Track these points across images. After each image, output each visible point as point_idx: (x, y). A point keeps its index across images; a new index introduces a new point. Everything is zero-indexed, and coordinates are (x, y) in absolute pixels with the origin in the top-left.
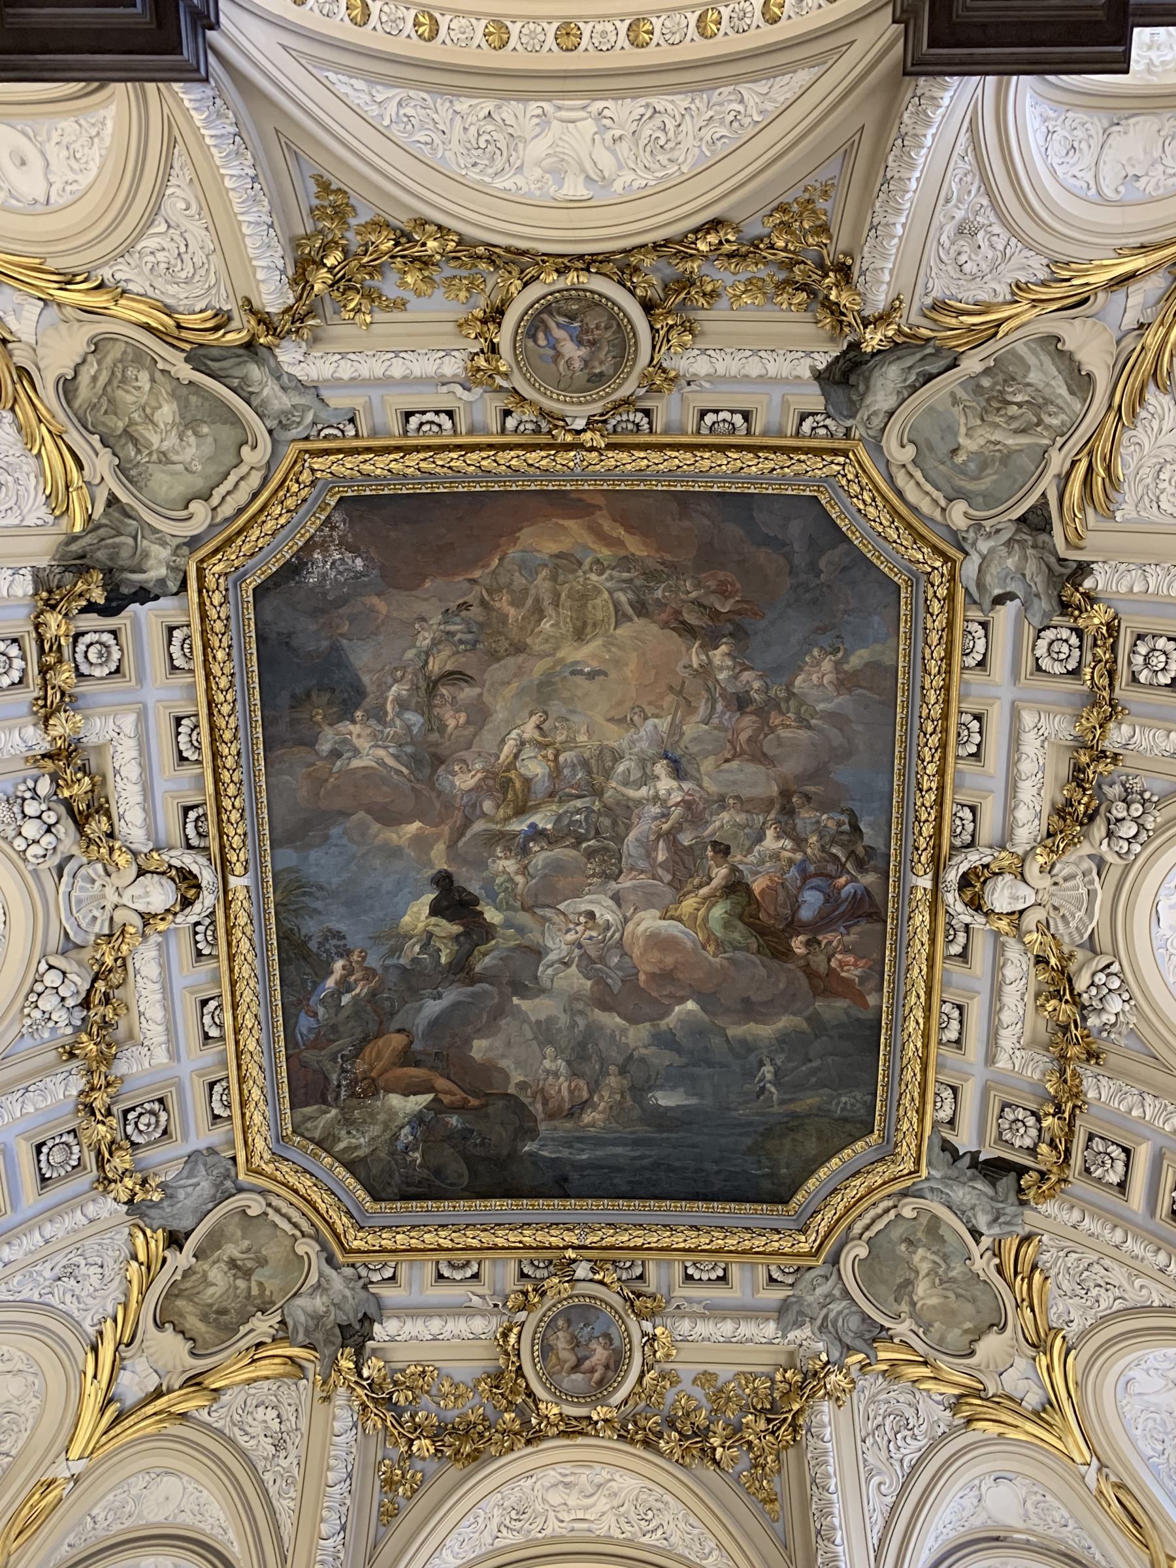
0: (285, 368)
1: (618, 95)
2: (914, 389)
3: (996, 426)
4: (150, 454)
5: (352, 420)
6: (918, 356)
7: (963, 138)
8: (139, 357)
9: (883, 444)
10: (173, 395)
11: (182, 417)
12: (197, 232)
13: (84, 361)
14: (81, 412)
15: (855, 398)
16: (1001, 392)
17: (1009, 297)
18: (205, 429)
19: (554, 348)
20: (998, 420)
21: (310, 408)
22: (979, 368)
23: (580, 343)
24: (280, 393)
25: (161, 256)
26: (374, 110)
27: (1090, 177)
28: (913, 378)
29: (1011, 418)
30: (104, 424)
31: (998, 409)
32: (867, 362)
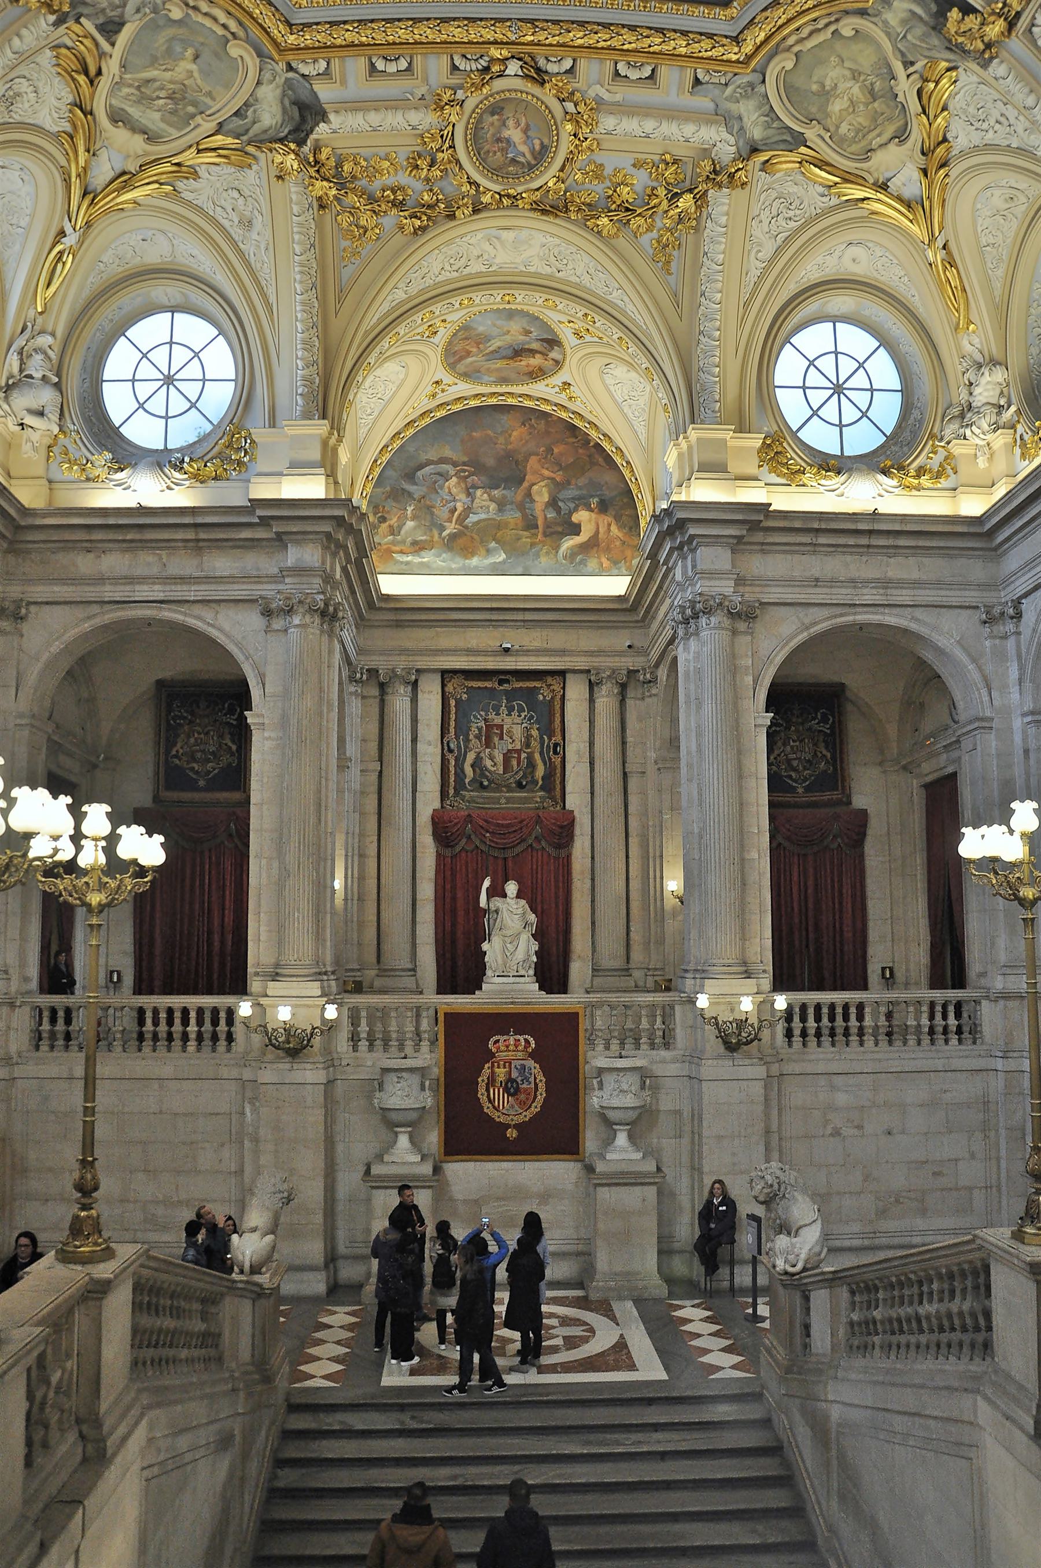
0: (732, 141)
1: (479, 274)
2: (247, 105)
3: (171, 82)
4: (865, 80)
5: (697, 82)
6: (251, 133)
7: (272, 299)
8: (839, 142)
9: (258, 60)
10: (828, 115)
11: (828, 101)
12: (758, 231)
13: (881, 146)
14: (902, 116)
15: (290, 92)
16: (176, 104)
17: (198, 169)
18: (815, 87)
19: (528, 137)
20: (172, 86)
21: (726, 99)
22: (199, 119)
23: (508, 141)
24: (745, 116)
25: (791, 214)
26: (626, 299)
27: (175, 242)
28: (249, 113)
29: (162, 89)
30: (888, 106)
31: (174, 93)
32: (289, 133)
